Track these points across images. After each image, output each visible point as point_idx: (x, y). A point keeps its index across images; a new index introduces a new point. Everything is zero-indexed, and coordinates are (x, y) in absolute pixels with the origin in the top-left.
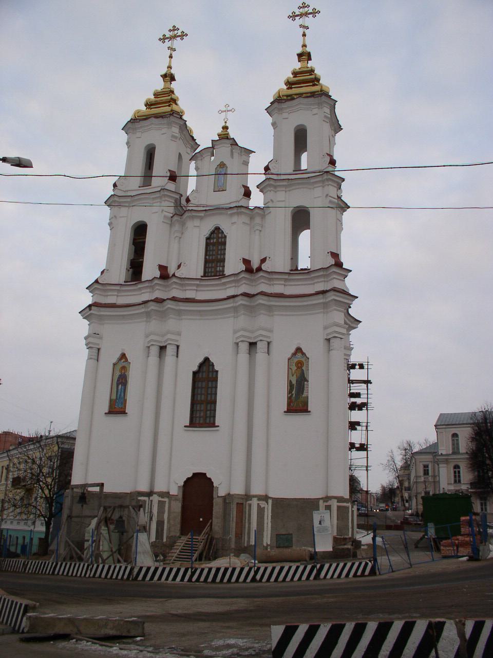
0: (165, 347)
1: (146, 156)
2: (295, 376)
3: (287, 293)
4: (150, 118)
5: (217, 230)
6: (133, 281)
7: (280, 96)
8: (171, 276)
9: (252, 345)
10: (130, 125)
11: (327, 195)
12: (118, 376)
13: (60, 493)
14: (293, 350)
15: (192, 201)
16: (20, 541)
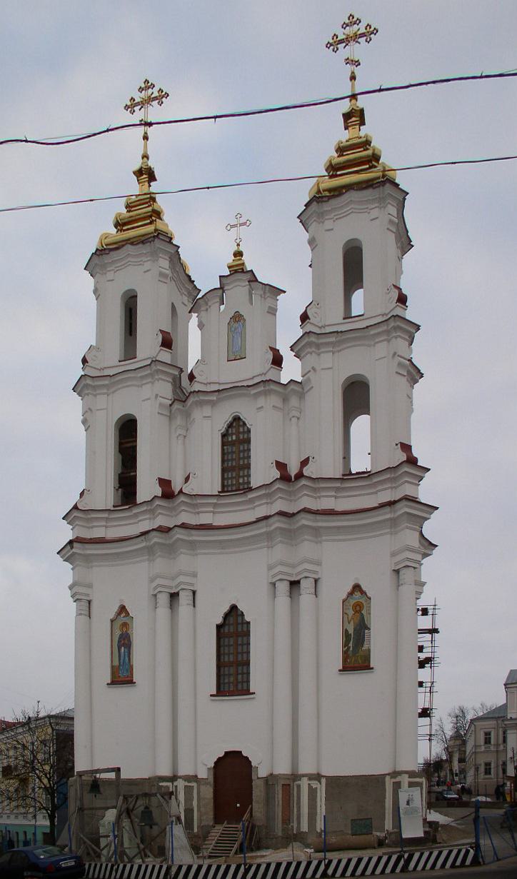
0: (177, 594)
1: (124, 308)
2: (352, 622)
3: (339, 508)
4: (123, 246)
5: (237, 421)
6: (127, 505)
7: (319, 192)
8: (176, 493)
9: (295, 584)
10: (96, 259)
11: (395, 354)
12: (118, 636)
13: (62, 782)
14: (349, 588)
15: (198, 378)
16: (21, 837)
